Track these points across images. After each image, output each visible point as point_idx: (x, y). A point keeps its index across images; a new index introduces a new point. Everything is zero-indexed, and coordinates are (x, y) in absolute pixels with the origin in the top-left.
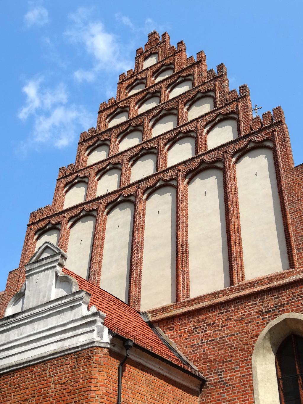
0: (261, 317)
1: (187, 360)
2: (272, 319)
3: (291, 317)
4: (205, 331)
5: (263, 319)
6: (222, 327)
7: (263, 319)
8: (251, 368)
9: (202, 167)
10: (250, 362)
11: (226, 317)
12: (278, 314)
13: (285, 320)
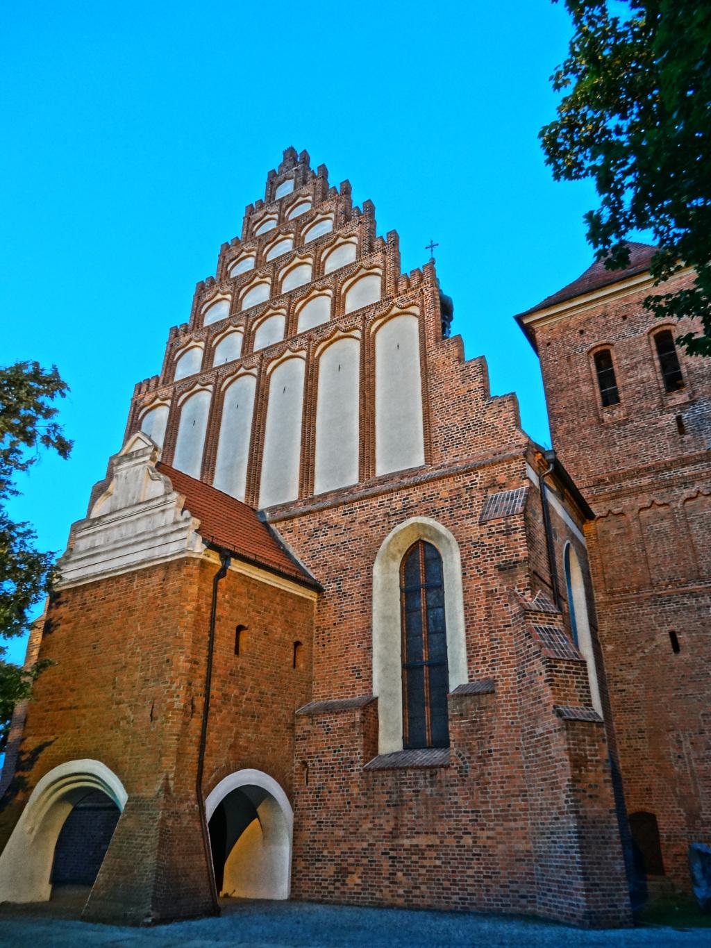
0: (387, 521)
1: (305, 568)
2: (399, 523)
3: (419, 522)
4: (326, 535)
5: (389, 522)
6: (345, 530)
7: (389, 522)
8: (371, 577)
9: (336, 336)
10: (371, 570)
11: (350, 519)
12: (405, 518)
13: (412, 525)
